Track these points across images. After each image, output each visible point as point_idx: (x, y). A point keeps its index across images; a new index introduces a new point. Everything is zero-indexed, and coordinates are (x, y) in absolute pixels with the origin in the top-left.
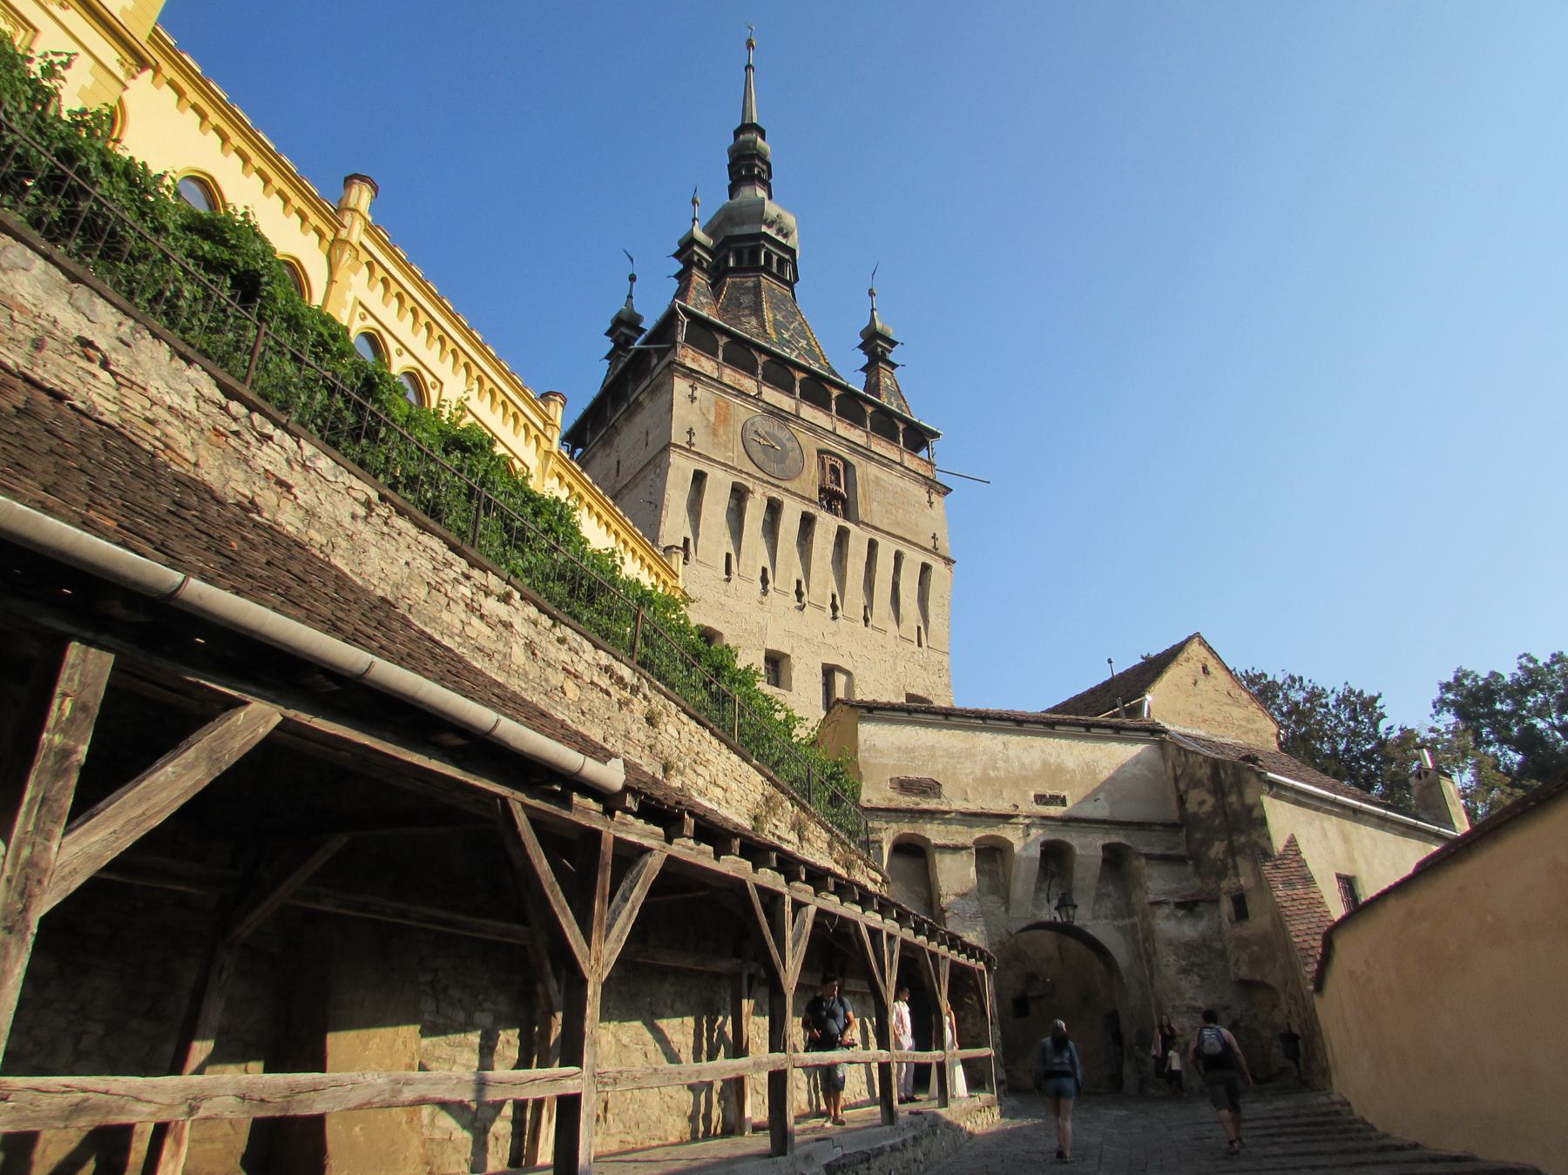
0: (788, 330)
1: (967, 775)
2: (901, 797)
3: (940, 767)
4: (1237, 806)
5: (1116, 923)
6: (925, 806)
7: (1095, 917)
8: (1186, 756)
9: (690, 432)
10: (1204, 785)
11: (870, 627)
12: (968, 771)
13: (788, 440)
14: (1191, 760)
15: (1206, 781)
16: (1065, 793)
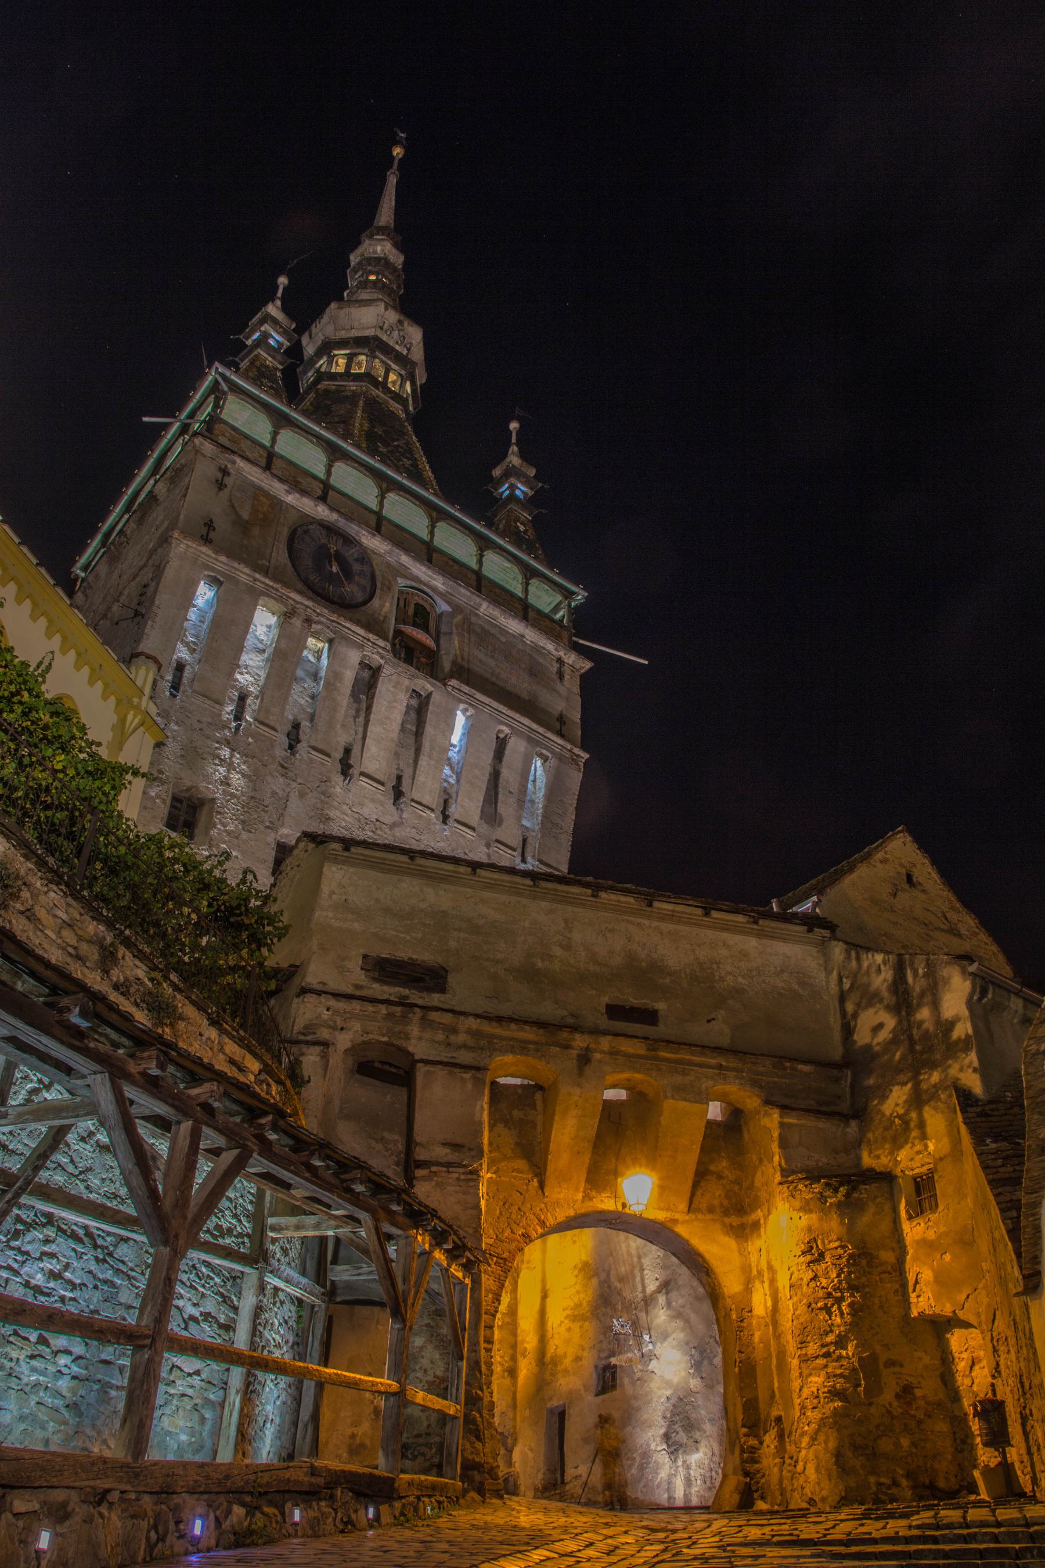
0: (386, 444)
1: (497, 962)
2: (376, 986)
3: (453, 944)
4: (929, 1026)
5: (727, 1220)
6: (420, 1002)
7: (690, 1209)
8: (858, 959)
9: (210, 525)
10: (881, 1001)
11: (451, 821)
12: (500, 956)
13: (356, 560)
14: (865, 964)
15: (885, 994)
16: (661, 1006)
